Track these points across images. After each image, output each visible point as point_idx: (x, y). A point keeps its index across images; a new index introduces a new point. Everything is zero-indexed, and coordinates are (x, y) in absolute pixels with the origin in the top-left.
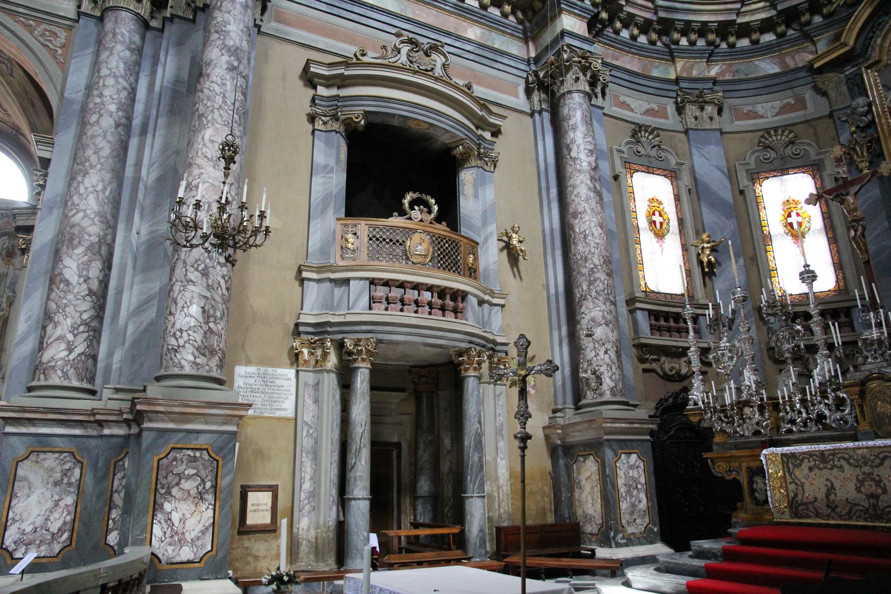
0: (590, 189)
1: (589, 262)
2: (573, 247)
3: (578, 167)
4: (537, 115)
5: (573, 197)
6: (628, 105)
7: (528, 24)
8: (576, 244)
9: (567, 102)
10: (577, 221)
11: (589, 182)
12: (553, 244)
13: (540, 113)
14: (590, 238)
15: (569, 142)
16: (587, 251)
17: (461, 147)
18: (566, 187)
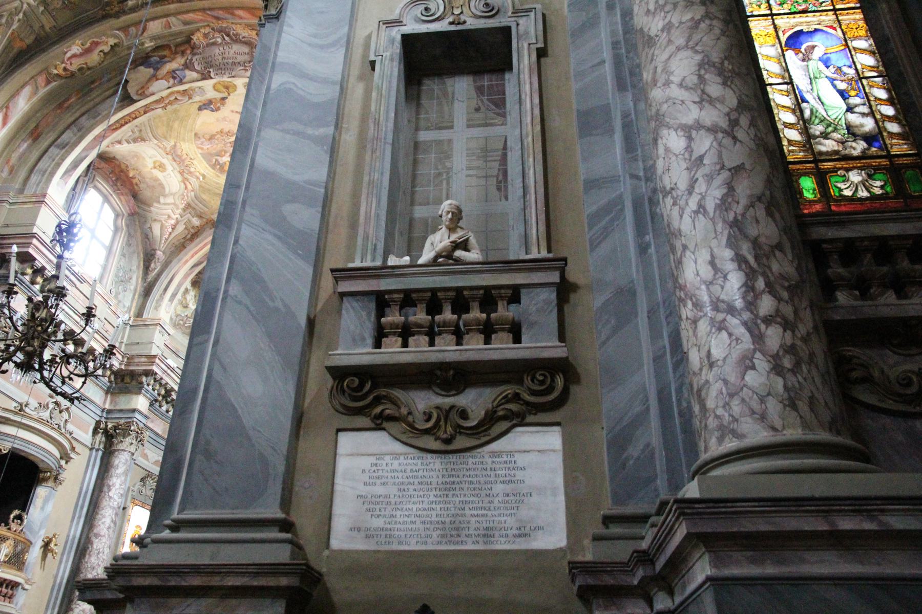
0: (112, 521)
1: (95, 571)
2: (87, 556)
3: (111, 504)
4: (94, 451)
5: (100, 523)
6: (147, 456)
7: (114, 385)
8: (90, 555)
9: (120, 456)
10: (97, 540)
11: (113, 516)
12: (71, 548)
13: (97, 450)
14: (101, 554)
15: (111, 484)
16: (97, 562)
17: (49, 474)
18: (97, 513)
